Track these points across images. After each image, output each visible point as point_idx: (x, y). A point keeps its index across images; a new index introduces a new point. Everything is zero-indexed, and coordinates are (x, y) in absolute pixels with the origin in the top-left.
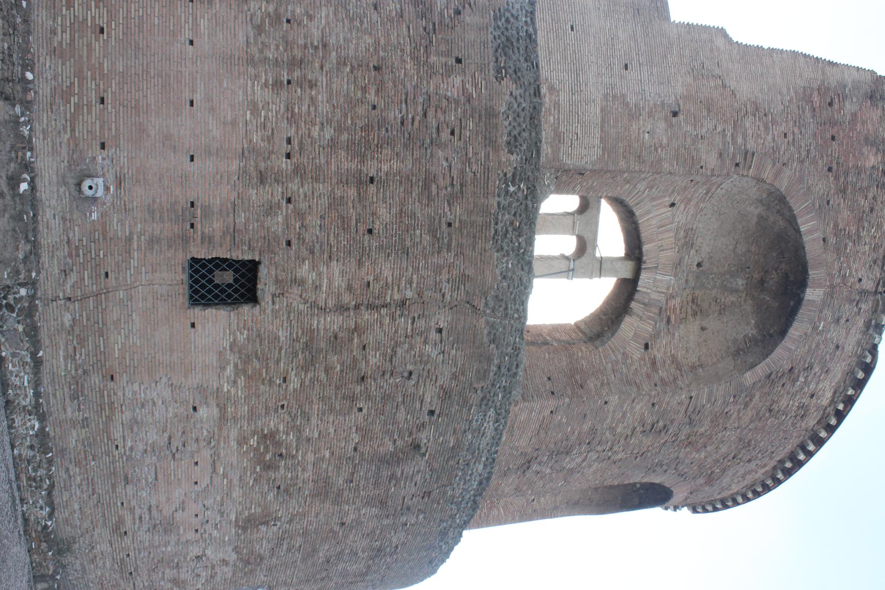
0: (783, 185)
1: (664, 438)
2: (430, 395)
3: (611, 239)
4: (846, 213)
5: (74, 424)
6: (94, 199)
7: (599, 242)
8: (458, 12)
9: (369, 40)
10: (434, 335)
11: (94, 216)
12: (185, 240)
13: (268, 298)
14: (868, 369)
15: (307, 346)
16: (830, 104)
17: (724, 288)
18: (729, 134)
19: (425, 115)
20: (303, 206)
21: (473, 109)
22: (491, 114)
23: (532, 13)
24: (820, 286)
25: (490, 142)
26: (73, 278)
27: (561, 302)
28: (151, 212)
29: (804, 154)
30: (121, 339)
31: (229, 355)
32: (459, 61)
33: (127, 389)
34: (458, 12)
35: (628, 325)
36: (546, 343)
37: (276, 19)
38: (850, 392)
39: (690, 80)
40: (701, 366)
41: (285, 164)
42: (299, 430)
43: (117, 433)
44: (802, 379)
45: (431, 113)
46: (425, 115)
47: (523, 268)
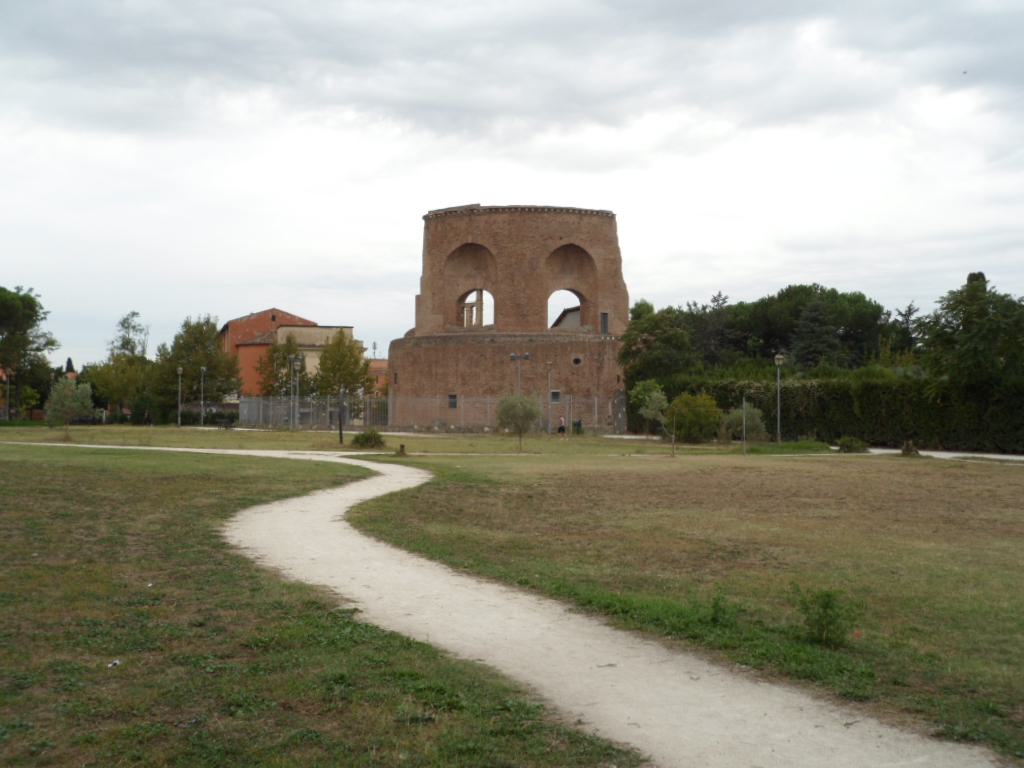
0: (445, 258)
3: (472, 298)
44: (499, 231)
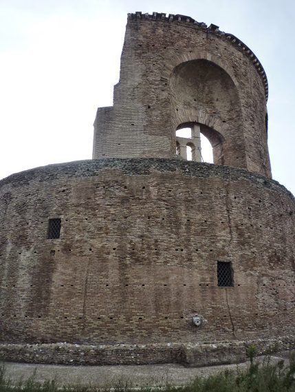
0: (172, 67)
1: (255, 117)
2: (254, 201)
3: (185, 133)
4: (180, 43)
5: (271, 328)
6: (201, 321)
7: (188, 137)
8: (125, 187)
9: (138, 220)
10: (237, 199)
11: (206, 320)
12: (213, 287)
13: (229, 258)
14: (233, 37)
15: (243, 245)
16: (141, 46)
17: (203, 91)
18: (155, 87)
19: (164, 201)
20: (199, 245)
21: (161, 183)
22: (162, 177)
23: (121, 159)
24: (206, 54)
25: (172, 177)
26: (226, 328)
27: (208, 153)
28: (204, 300)
29: (160, 58)
30: (245, 311)
31: (248, 272)
32: (144, 188)
33: (260, 310)
34: (125, 187)
35: (217, 128)
36: (222, 158)
37: (132, 254)
38: (240, 45)
39: (136, 100)
40: (231, 101)
41: (184, 252)
42: (268, 248)
43: (272, 313)
45: (164, 198)
46: (164, 201)
47: (198, 166)
